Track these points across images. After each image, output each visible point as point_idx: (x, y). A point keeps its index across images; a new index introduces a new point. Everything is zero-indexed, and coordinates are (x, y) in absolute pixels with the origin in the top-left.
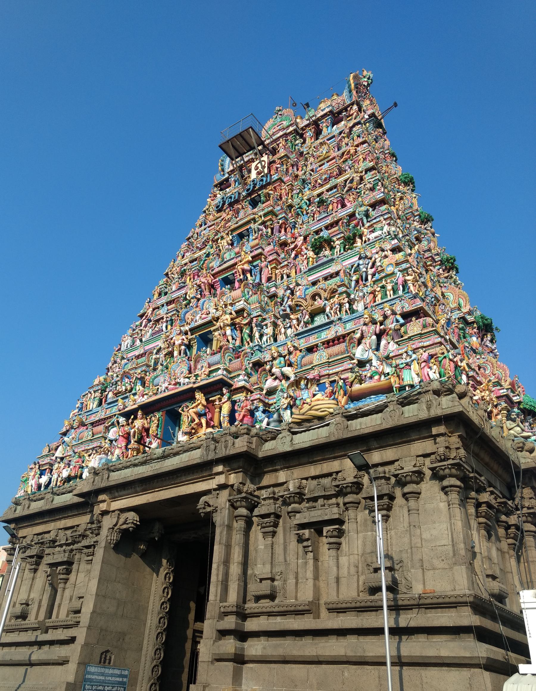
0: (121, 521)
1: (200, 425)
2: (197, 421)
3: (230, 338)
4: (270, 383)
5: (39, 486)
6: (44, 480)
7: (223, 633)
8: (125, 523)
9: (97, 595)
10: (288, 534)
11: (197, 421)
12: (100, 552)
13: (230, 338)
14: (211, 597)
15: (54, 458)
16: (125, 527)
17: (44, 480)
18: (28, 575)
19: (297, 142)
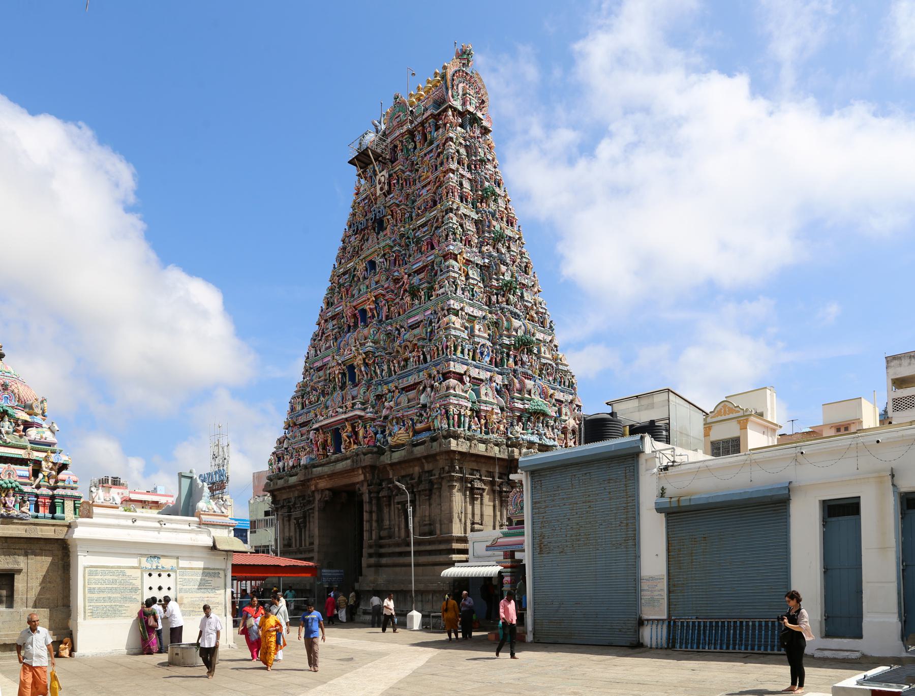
0: (324, 496)
1: (350, 442)
2: (348, 441)
3: (364, 373)
4: (385, 412)
5: (279, 469)
6: (281, 464)
7: (370, 555)
8: (325, 497)
9: (319, 536)
10: (386, 510)
11: (348, 441)
12: (316, 514)
13: (364, 373)
14: (365, 538)
15: (283, 449)
16: (326, 499)
17: (281, 464)
18: (287, 523)
19: (410, 147)
